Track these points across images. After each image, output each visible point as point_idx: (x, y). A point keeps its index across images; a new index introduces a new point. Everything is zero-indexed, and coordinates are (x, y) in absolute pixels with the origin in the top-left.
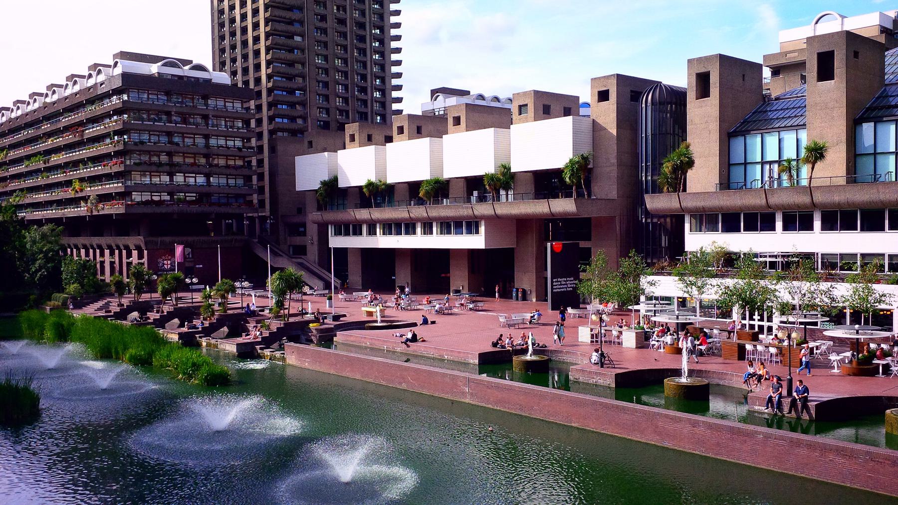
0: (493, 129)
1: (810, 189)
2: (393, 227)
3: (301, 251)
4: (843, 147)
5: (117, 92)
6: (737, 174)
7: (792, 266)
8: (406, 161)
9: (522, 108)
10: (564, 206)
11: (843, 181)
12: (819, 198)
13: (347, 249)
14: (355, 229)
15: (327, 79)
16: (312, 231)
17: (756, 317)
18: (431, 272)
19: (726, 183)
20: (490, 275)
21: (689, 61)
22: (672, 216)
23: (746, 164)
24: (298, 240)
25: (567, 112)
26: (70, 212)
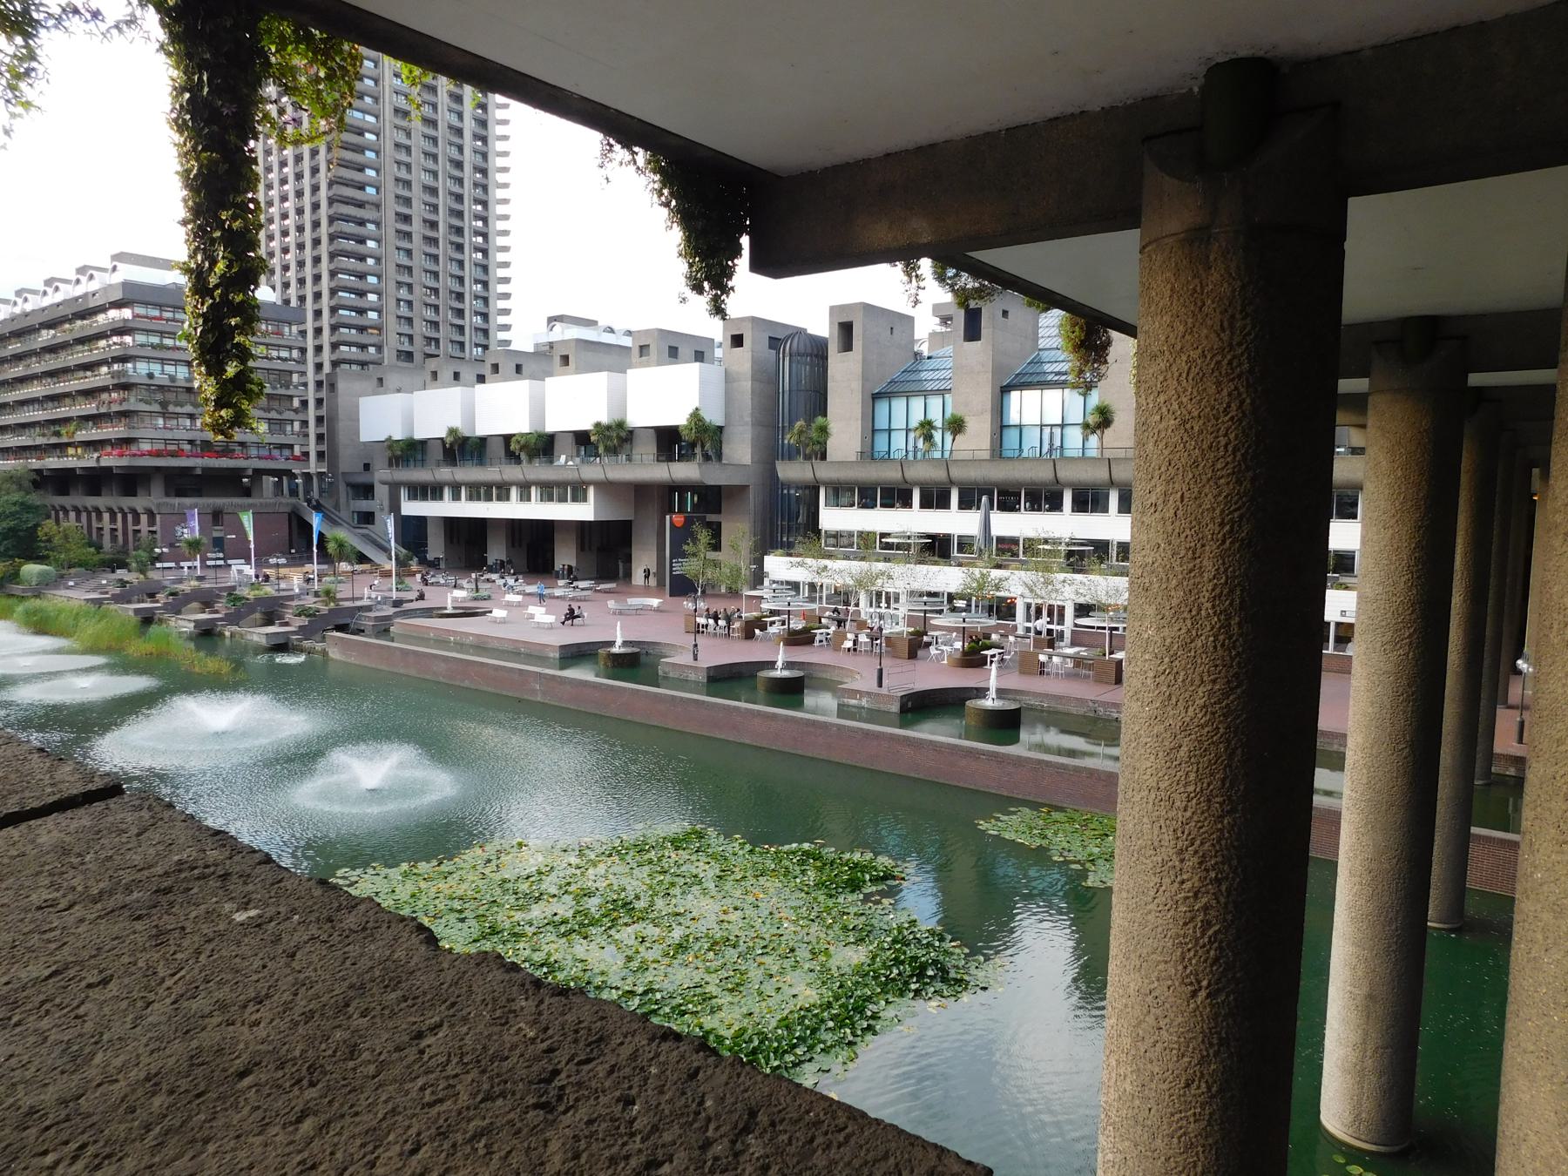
0: (604, 374)
1: (946, 464)
2: (479, 491)
3: (367, 518)
4: (988, 417)
5: (118, 305)
6: (881, 443)
7: (937, 548)
8: (501, 409)
9: (643, 349)
10: (685, 471)
11: (986, 455)
12: (956, 473)
13: (424, 518)
14: (431, 491)
15: (409, 298)
16: (381, 492)
17: (883, 604)
18: (533, 549)
19: (869, 454)
20: (605, 551)
21: (832, 308)
22: (807, 487)
23: (890, 431)
24: (364, 505)
25: (699, 356)
26: (53, 462)
